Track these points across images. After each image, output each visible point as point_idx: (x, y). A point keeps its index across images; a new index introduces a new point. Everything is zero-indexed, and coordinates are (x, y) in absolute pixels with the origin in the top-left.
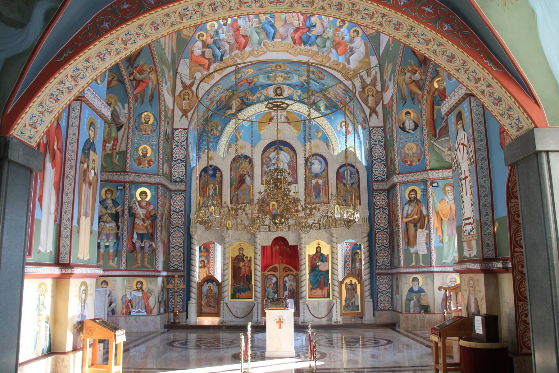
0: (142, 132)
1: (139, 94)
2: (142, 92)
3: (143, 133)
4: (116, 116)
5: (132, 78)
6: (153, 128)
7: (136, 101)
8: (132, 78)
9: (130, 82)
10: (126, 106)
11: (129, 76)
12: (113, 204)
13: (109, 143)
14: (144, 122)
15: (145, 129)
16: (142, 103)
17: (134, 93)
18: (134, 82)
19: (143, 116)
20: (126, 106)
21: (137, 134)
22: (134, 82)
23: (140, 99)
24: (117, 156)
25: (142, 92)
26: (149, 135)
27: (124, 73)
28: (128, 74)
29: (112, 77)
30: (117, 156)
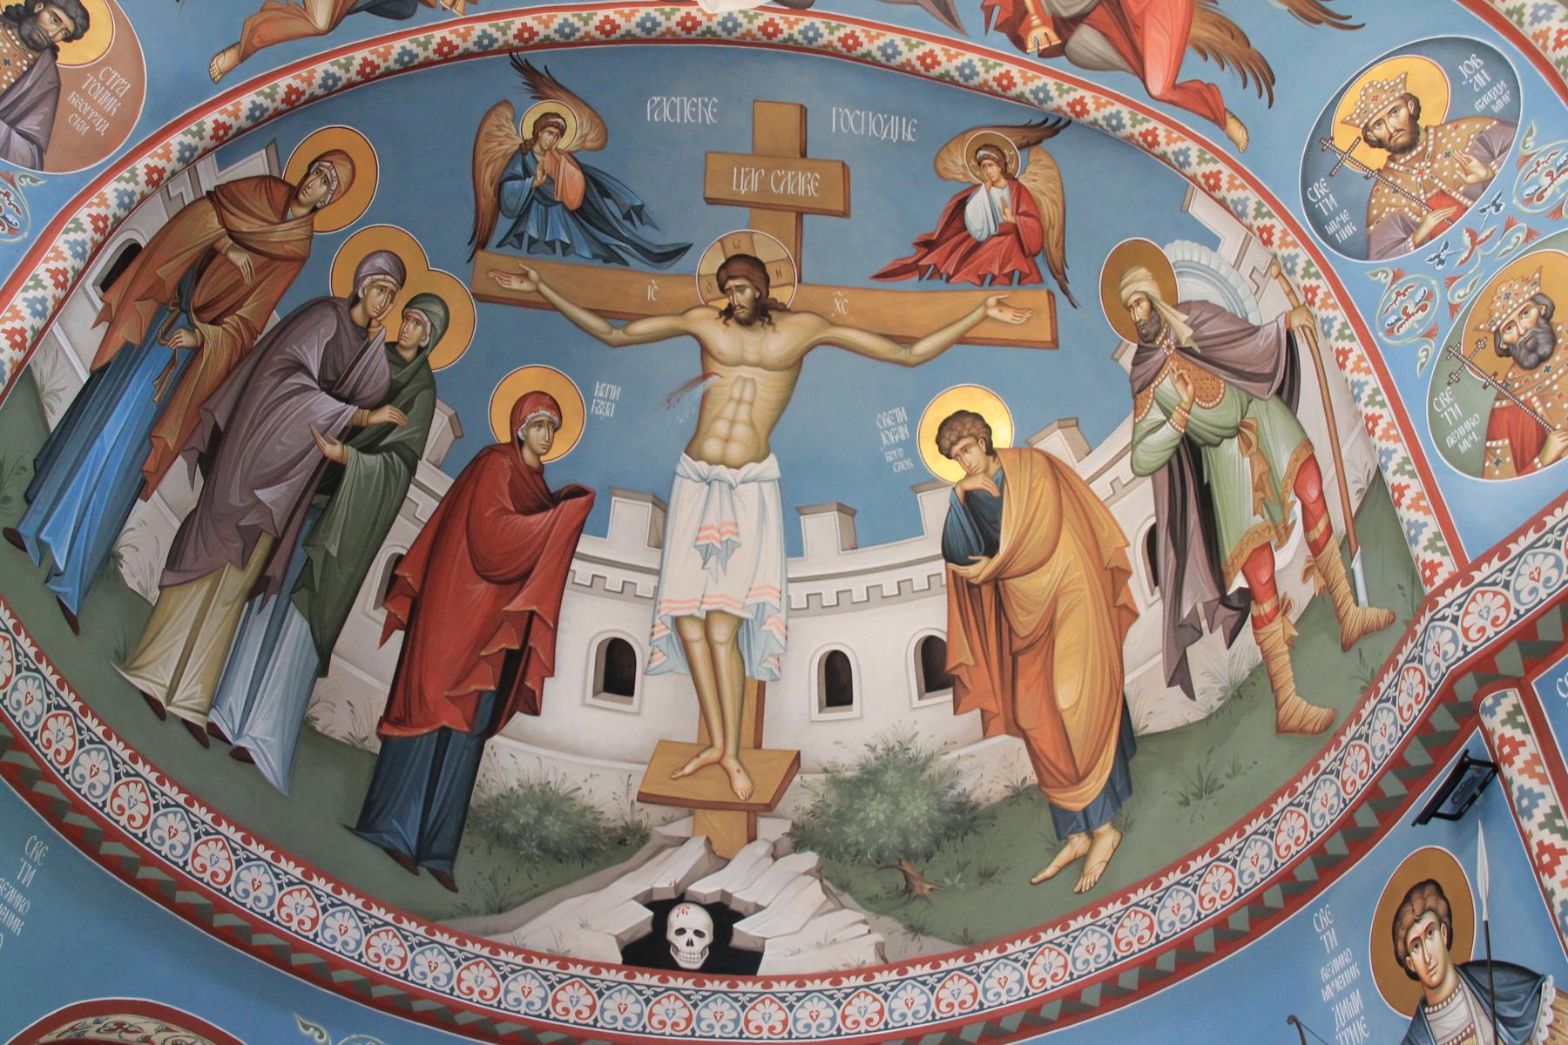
0: (1410, 228)
1: (1192, 56)
2: (1199, 31)
3: (1432, 221)
4: (1232, 339)
5: (1040, 35)
6: (1487, 115)
7: (1218, 117)
8: (1040, 35)
9: (1060, 64)
10: (1202, 209)
11: (1020, 43)
12: (1495, 1017)
13: (1284, 532)
14: (1378, 158)
15: (1427, 185)
16: (1265, 77)
17: (1157, 85)
18: (1087, 39)
19: (1343, 137)
20: (1202, 209)
21: (1384, 278)
22: (1087, 39)
23: (1225, 80)
24: (1357, 565)
25: (1199, 31)
26: (1484, 184)
27: (950, 62)
28: (1000, 42)
29: (994, 171)
30: (1357, 565)
